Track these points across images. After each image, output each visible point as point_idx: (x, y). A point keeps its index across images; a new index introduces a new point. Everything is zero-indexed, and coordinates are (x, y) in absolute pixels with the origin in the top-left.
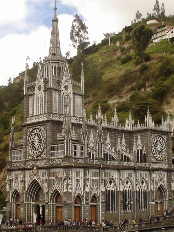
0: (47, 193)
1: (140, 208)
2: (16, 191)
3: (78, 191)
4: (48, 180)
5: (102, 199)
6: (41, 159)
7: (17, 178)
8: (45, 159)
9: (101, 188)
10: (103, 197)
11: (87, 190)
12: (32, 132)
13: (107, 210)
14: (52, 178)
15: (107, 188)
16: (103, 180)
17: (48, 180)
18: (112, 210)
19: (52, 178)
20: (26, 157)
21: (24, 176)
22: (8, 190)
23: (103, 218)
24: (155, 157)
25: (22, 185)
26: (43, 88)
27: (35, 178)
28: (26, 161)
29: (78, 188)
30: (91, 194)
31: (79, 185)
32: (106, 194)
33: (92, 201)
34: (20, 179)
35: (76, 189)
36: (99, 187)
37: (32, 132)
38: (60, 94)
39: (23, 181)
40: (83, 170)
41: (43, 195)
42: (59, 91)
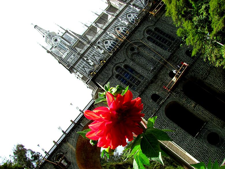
3: (88, 70)
11: (92, 64)
29: (86, 70)
31: (86, 67)
35: (86, 72)
36: (100, 54)
40: (81, 60)
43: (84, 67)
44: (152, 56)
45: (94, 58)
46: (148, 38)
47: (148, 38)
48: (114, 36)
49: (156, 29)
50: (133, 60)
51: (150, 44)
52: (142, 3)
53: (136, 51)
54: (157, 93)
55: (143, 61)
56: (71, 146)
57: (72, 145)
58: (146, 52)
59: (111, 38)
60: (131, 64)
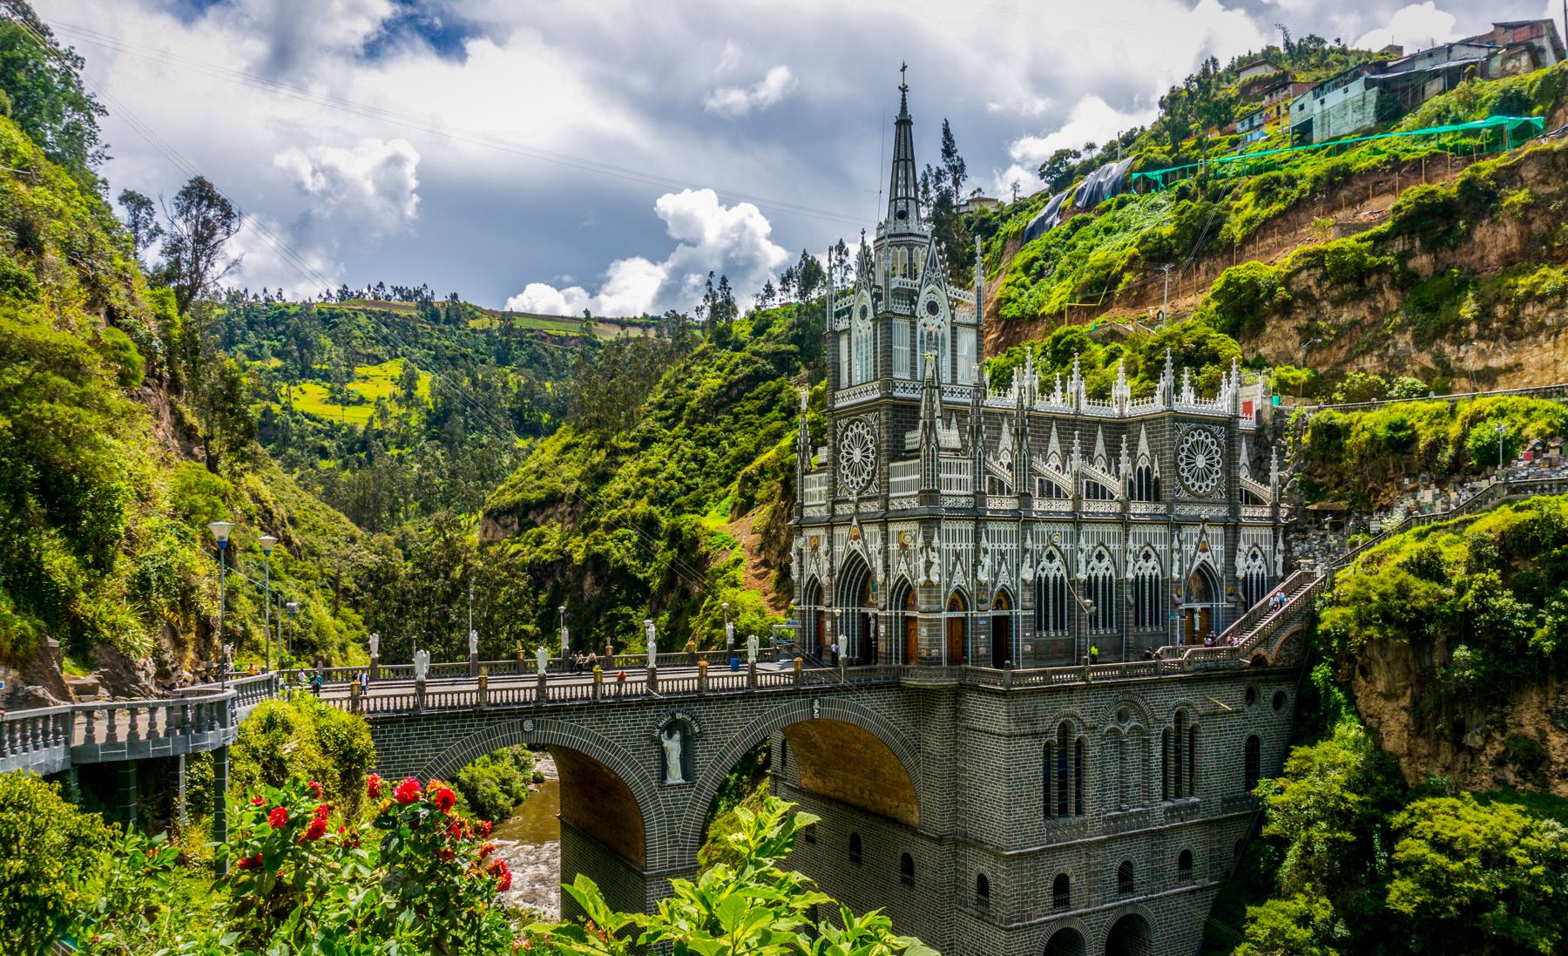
0: (884, 584)
1: (1137, 624)
2: (814, 581)
3: (959, 580)
4: (886, 553)
5: (1025, 597)
6: (869, 499)
7: (815, 548)
8: (875, 498)
9: (1022, 571)
10: (1028, 595)
11: (983, 577)
12: (846, 429)
13: (1040, 628)
14: (894, 547)
15: (1039, 571)
16: (1026, 551)
17: (886, 553)
18: (1055, 628)
19: (894, 547)
20: (834, 494)
21: (831, 542)
22: (795, 577)
23: (1028, 648)
24: (1187, 489)
25: (827, 566)
26: (870, 315)
27: (856, 546)
28: (835, 503)
30: (994, 585)
32: (1039, 586)
33: (998, 605)
34: (823, 547)
35: (951, 575)
37: (846, 429)
38: (913, 328)
39: (830, 553)
41: (875, 589)
43: (958, 555)
44: (1135, 778)
45: (1000, 564)
48: (1082, 566)
49: (1193, 731)
52: (1192, 561)
54: (1073, 880)
59: (1070, 564)
60: (1093, 751)
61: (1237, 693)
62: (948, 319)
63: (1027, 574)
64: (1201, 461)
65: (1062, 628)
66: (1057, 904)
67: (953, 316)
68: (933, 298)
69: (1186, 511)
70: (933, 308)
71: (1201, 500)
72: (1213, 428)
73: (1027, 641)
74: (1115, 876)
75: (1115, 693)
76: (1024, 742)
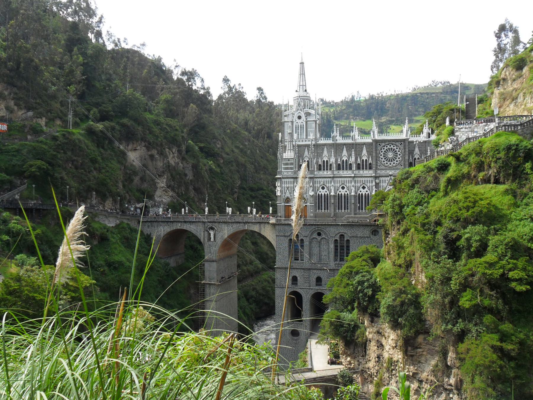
18: (325, 209)
35: (285, 193)
38: (292, 124)
40: (292, 180)
42: (292, 122)
43: (288, 188)
44: (324, 253)
46: (336, 241)
47: (336, 240)
48: (333, 191)
49: (348, 241)
50: (310, 243)
51: (332, 246)
53: (319, 238)
54: (299, 278)
55: (316, 250)
56: (226, 231)
57: (228, 231)
58: (324, 247)
60: (306, 243)
61: (367, 232)
62: (305, 120)
63: (312, 193)
64: (390, 155)
65: (328, 209)
66: (292, 284)
67: (306, 119)
68: (300, 115)
69: (383, 172)
70: (299, 117)
71: (390, 168)
72: (397, 144)
73: (311, 212)
74: (314, 280)
75: (314, 227)
76: (283, 238)
